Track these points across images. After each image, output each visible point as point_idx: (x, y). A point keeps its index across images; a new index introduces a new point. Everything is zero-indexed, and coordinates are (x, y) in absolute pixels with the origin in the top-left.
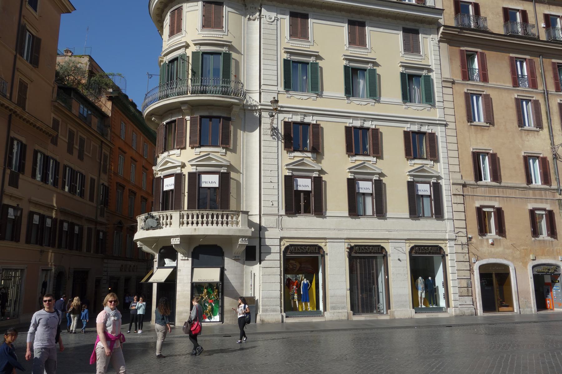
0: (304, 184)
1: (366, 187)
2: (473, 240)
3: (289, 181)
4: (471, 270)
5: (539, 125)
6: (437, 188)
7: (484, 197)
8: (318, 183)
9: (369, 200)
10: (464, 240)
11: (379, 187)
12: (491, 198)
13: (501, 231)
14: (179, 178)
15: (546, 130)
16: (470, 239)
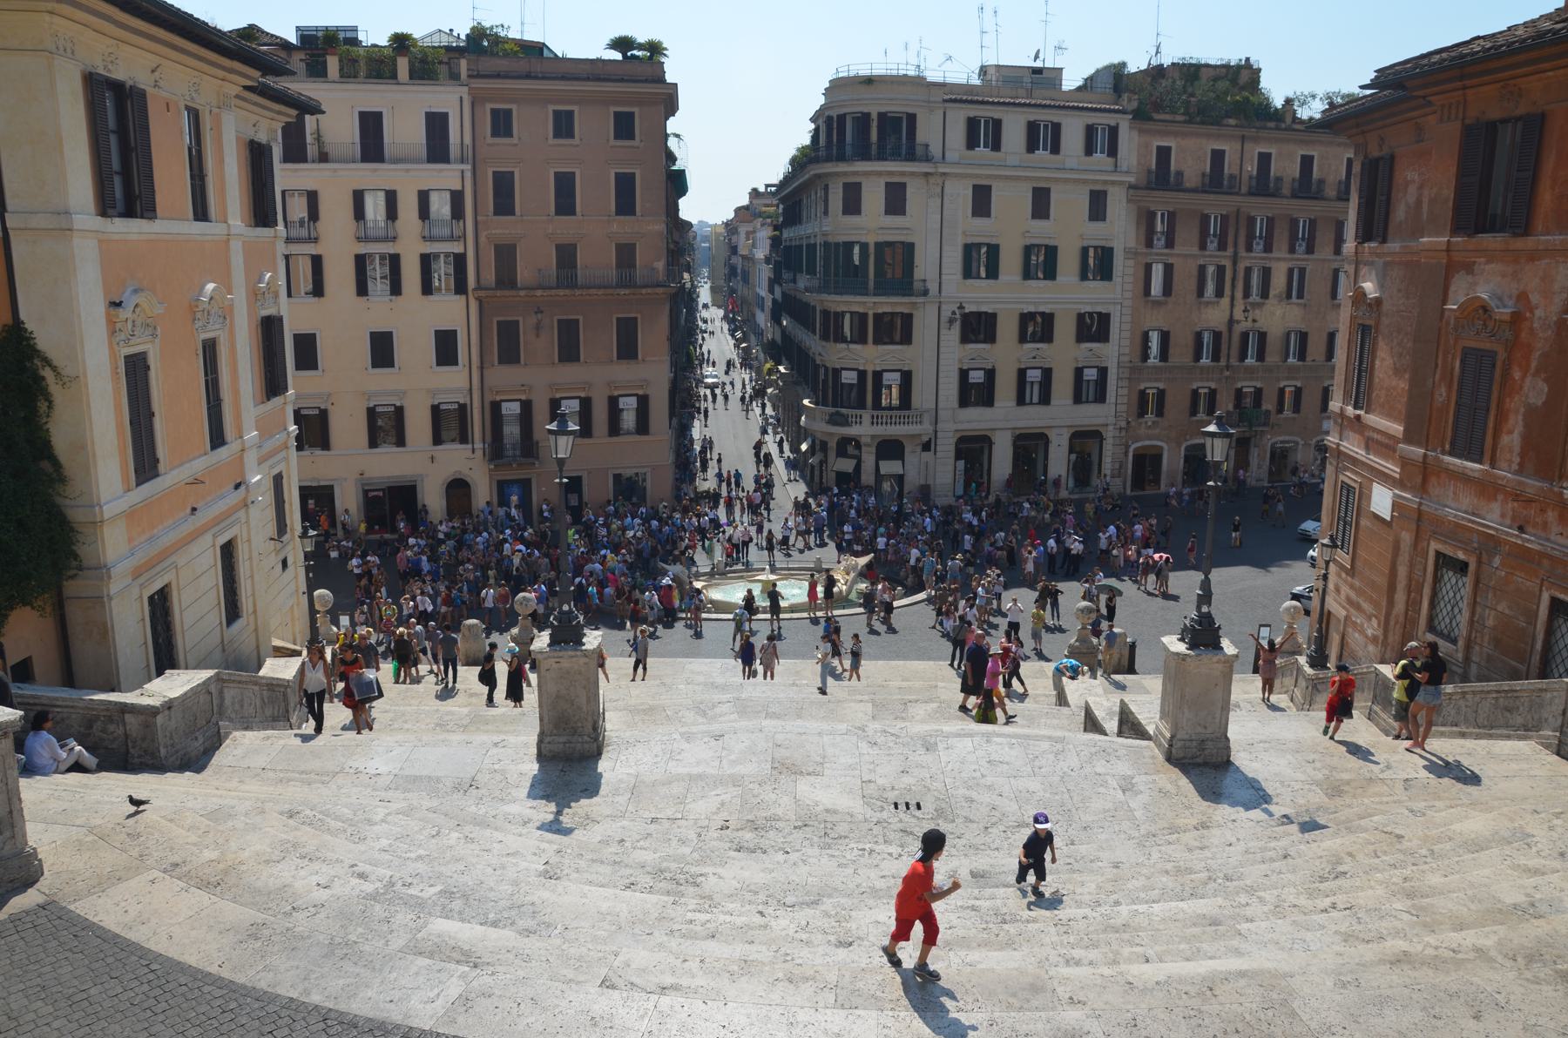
0: (976, 377)
1: (1034, 375)
2: (1133, 424)
3: (964, 374)
4: (1126, 453)
5: (1219, 293)
6: (1103, 372)
7: (1150, 380)
8: (991, 374)
9: (1036, 388)
10: (1123, 424)
11: (1047, 373)
12: (1156, 380)
13: (1160, 413)
14: (862, 374)
15: (1226, 301)
16: (1128, 423)
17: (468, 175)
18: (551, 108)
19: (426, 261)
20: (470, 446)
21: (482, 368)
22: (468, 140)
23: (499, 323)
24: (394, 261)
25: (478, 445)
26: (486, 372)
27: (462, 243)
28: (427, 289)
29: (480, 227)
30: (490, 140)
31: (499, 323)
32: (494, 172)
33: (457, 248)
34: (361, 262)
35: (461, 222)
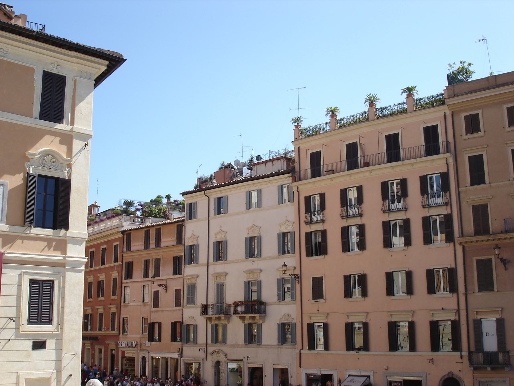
17: (451, 161)
18: (505, 107)
19: (426, 221)
20: (459, 353)
21: (466, 295)
22: (451, 139)
23: (478, 262)
24: (407, 223)
25: (465, 353)
26: (469, 297)
27: (449, 204)
28: (428, 240)
29: (462, 195)
30: (465, 136)
31: (478, 262)
32: (469, 157)
33: (445, 211)
34: (386, 225)
35: (448, 193)
